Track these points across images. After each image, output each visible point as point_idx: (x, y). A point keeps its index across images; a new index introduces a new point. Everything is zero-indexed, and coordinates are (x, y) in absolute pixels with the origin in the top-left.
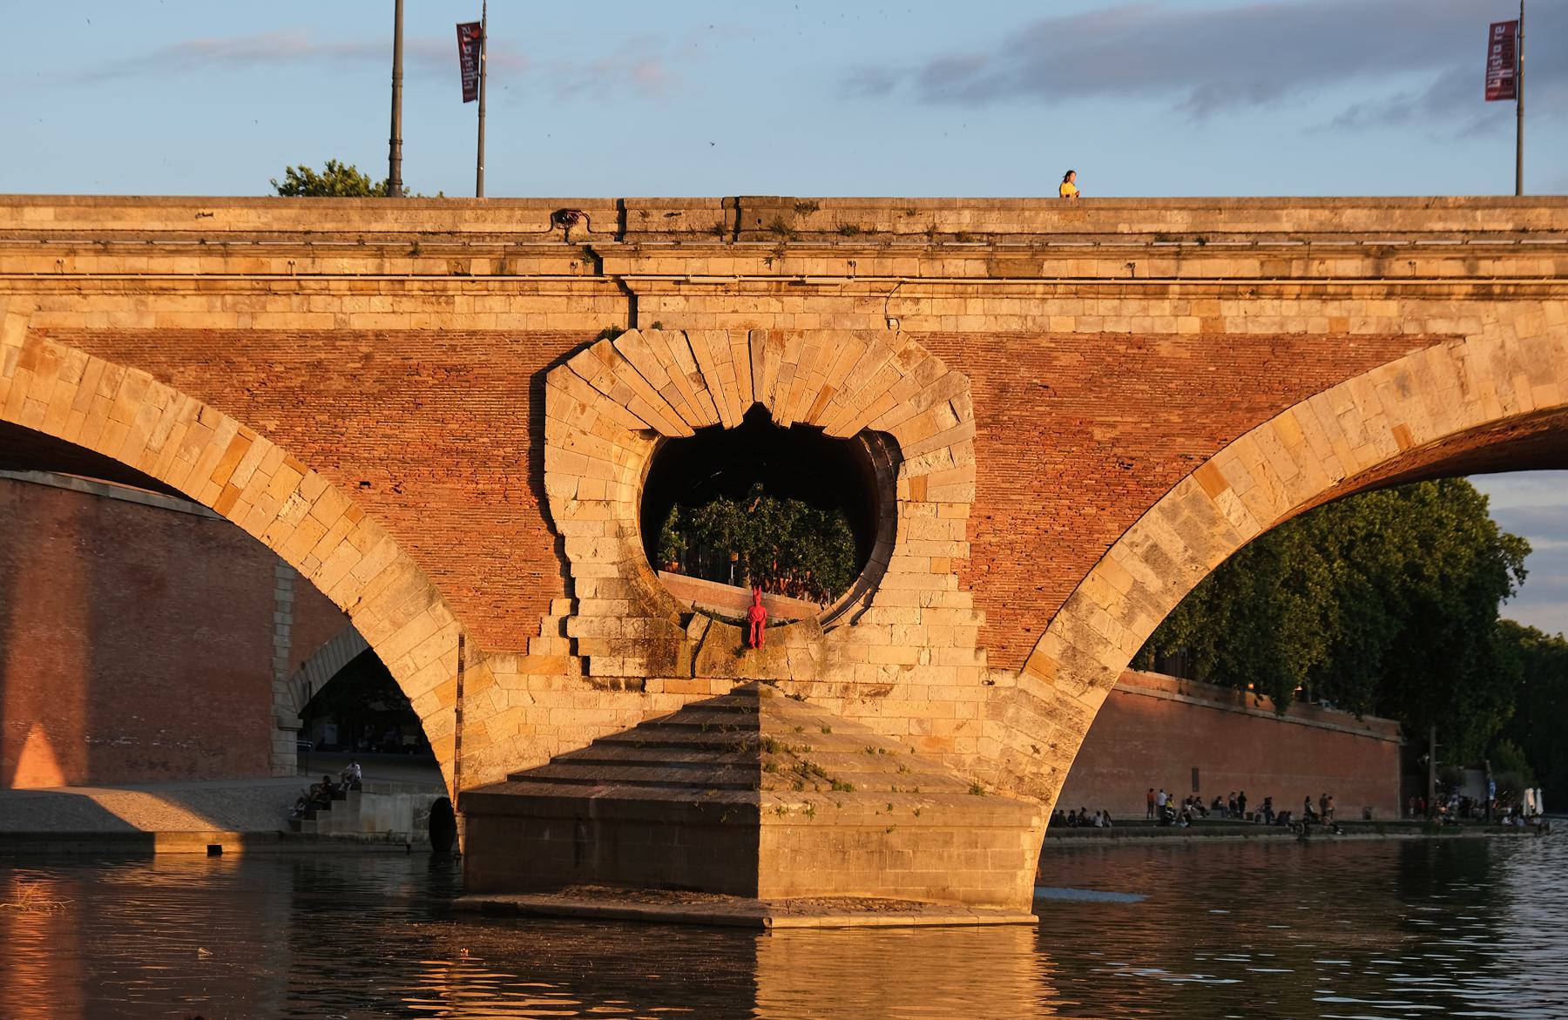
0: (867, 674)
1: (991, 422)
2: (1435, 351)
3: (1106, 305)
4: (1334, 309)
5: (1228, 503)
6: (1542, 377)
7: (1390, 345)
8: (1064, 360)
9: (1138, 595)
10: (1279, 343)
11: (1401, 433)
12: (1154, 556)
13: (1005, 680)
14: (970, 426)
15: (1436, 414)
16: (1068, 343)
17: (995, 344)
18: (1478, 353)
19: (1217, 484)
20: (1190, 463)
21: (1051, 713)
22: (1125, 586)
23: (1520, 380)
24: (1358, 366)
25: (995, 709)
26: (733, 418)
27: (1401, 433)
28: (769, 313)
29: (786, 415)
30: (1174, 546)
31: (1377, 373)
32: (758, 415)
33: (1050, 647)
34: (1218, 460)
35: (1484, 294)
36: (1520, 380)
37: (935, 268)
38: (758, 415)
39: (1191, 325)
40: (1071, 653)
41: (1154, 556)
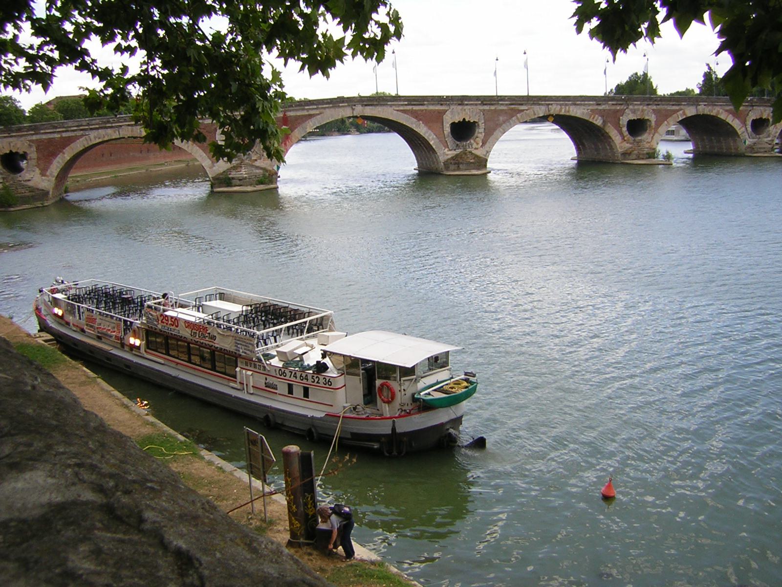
0: (27, 179)
1: (38, 149)
2: (87, 137)
3: (49, 135)
4: (75, 133)
5: (65, 155)
6: (99, 138)
7: (82, 136)
8: (46, 141)
9: (57, 167)
10: (69, 137)
11: (84, 146)
12: (58, 162)
13: (43, 178)
14: (35, 150)
15: (88, 143)
16: (45, 139)
17: (37, 140)
18: (92, 136)
19: (64, 153)
20: (60, 152)
21: (49, 181)
22: (55, 166)
23: (97, 139)
24: (78, 139)
25: (43, 180)
26: (8, 152)
27: (84, 146)
28: (11, 139)
29: (14, 151)
30: (61, 161)
31: (81, 140)
32: (11, 151)
33: (48, 173)
34: (64, 151)
35: (91, 129)
36: (97, 139)
37: (28, 133)
38: (11, 151)
39: (59, 136)
40: (51, 174)
41: (58, 162)
